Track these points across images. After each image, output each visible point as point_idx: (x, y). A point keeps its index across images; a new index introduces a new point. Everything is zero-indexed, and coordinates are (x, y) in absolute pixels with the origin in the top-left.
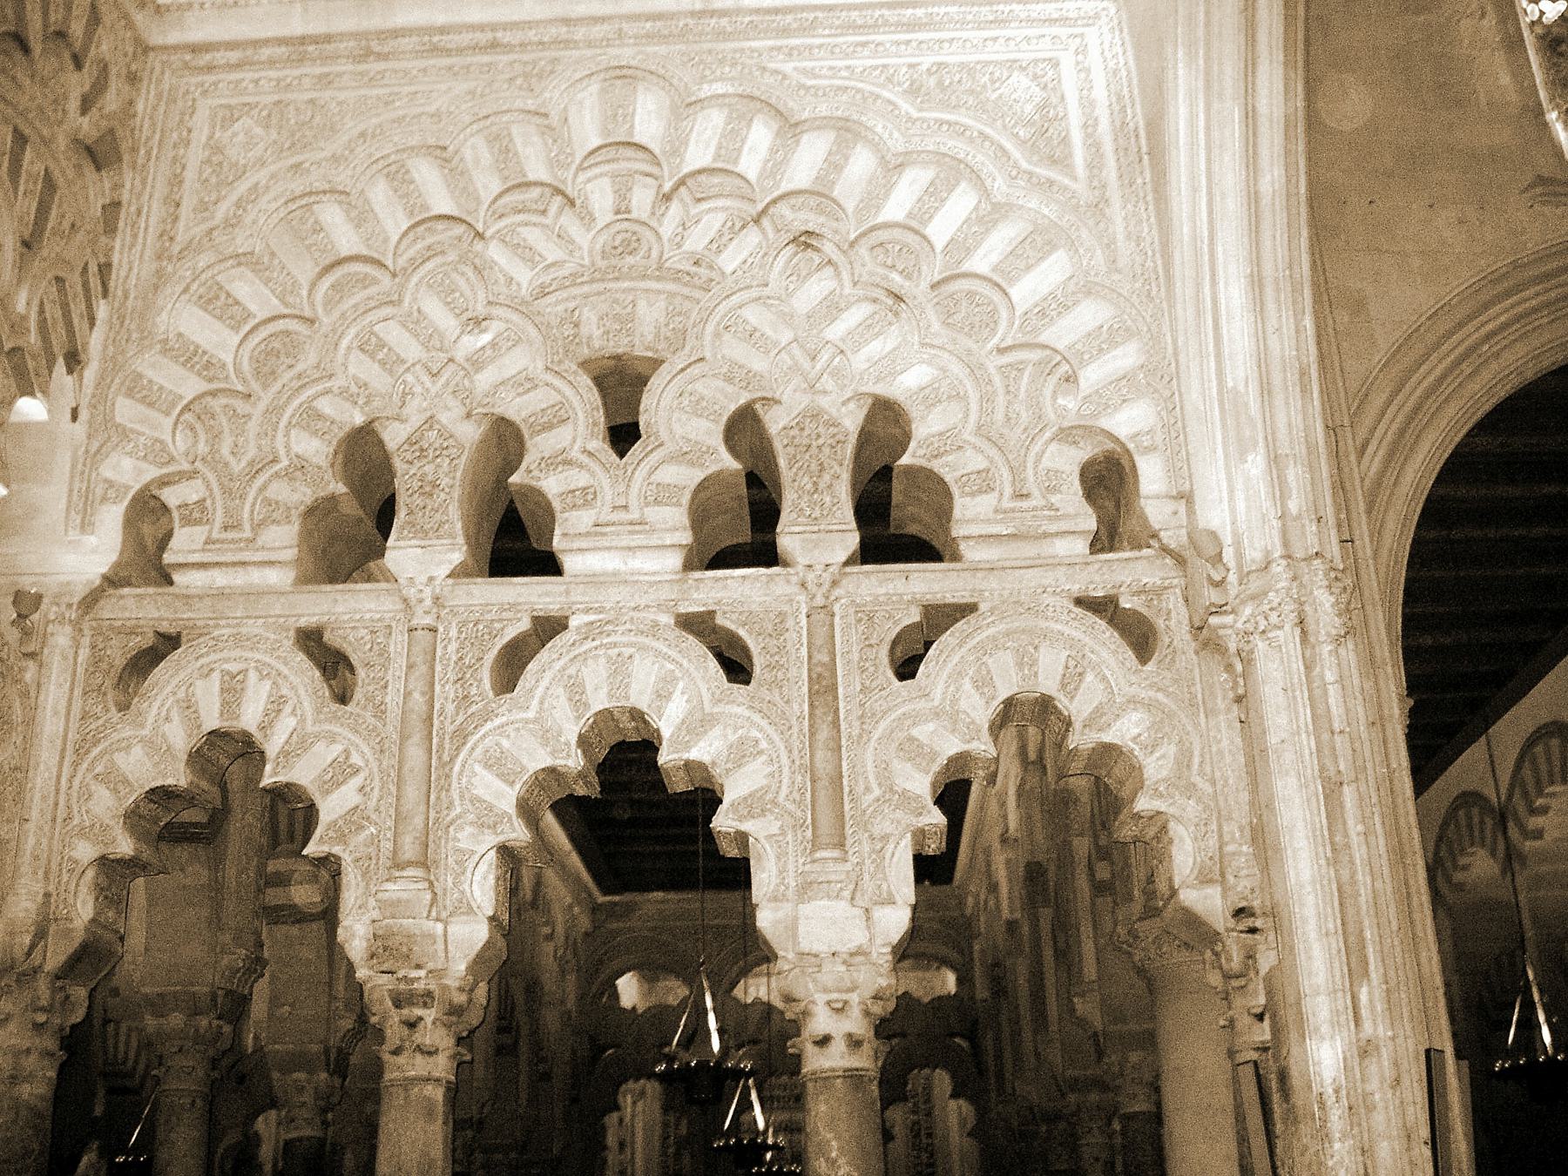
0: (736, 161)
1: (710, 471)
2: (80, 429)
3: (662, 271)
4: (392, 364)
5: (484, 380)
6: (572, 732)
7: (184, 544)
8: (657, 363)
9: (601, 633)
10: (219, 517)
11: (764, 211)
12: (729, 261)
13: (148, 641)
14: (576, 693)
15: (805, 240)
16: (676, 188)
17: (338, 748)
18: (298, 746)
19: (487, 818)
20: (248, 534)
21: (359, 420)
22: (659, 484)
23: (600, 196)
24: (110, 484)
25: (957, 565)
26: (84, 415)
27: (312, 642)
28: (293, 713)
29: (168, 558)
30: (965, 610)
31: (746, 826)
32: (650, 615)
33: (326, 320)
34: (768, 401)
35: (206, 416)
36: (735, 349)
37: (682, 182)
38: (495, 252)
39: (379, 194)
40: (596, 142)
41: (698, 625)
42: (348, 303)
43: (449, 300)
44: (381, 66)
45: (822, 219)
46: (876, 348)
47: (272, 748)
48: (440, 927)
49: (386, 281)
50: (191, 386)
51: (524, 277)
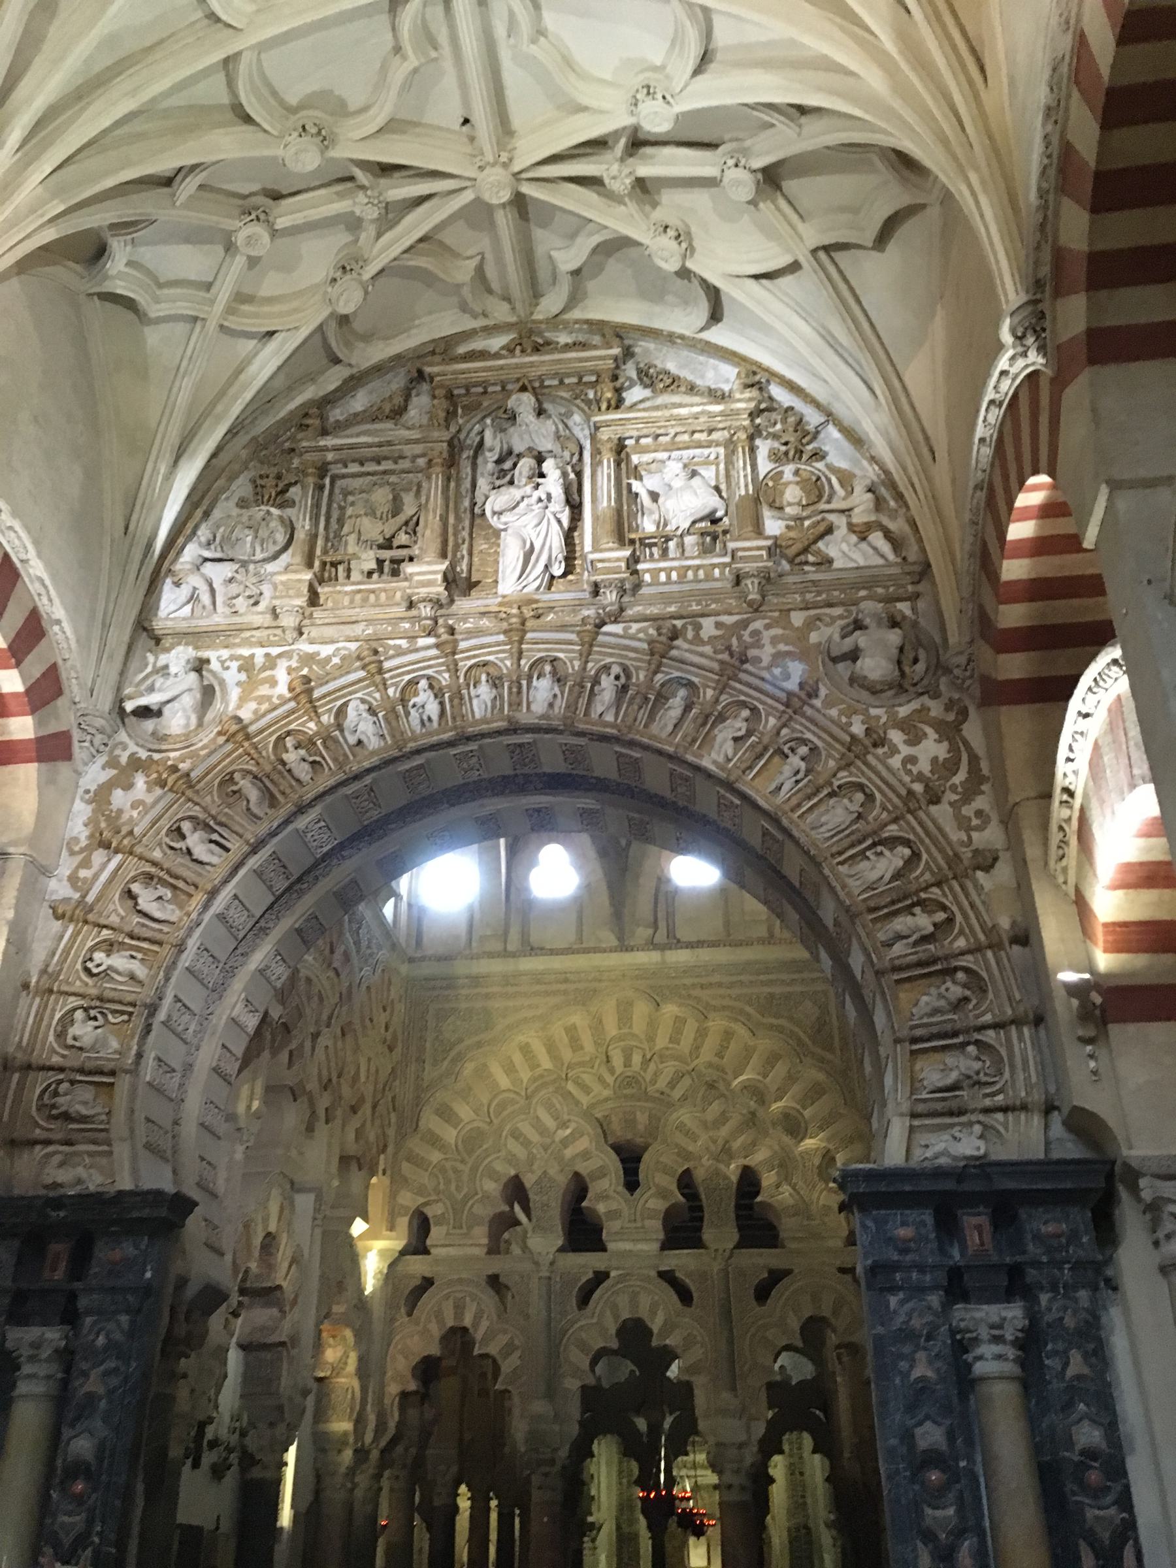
2: (386, 1180)
3: (646, 1097)
4: (526, 1143)
6: (613, 1331)
7: (436, 1234)
13: (418, 1282)
14: (615, 1308)
15: (711, 1086)
18: (489, 1336)
20: (464, 1231)
21: (513, 1173)
23: (618, 1061)
26: (388, 1172)
29: (429, 1242)
30: (788, 1273)
31: (693, 1379)
32: (645, 1272)
33: (495, 1121)
35: (443, 1170)
36: (680, 1139)
38: (570, 1086)
39: (517, 1058)
41: (667, 1277)
42: (505, 1113)
44: (515, 989)
47: (479, 1336)
48: (556, 1428)
49: (522, 1102)
50: (435, 1156)
51: (585, 1100)
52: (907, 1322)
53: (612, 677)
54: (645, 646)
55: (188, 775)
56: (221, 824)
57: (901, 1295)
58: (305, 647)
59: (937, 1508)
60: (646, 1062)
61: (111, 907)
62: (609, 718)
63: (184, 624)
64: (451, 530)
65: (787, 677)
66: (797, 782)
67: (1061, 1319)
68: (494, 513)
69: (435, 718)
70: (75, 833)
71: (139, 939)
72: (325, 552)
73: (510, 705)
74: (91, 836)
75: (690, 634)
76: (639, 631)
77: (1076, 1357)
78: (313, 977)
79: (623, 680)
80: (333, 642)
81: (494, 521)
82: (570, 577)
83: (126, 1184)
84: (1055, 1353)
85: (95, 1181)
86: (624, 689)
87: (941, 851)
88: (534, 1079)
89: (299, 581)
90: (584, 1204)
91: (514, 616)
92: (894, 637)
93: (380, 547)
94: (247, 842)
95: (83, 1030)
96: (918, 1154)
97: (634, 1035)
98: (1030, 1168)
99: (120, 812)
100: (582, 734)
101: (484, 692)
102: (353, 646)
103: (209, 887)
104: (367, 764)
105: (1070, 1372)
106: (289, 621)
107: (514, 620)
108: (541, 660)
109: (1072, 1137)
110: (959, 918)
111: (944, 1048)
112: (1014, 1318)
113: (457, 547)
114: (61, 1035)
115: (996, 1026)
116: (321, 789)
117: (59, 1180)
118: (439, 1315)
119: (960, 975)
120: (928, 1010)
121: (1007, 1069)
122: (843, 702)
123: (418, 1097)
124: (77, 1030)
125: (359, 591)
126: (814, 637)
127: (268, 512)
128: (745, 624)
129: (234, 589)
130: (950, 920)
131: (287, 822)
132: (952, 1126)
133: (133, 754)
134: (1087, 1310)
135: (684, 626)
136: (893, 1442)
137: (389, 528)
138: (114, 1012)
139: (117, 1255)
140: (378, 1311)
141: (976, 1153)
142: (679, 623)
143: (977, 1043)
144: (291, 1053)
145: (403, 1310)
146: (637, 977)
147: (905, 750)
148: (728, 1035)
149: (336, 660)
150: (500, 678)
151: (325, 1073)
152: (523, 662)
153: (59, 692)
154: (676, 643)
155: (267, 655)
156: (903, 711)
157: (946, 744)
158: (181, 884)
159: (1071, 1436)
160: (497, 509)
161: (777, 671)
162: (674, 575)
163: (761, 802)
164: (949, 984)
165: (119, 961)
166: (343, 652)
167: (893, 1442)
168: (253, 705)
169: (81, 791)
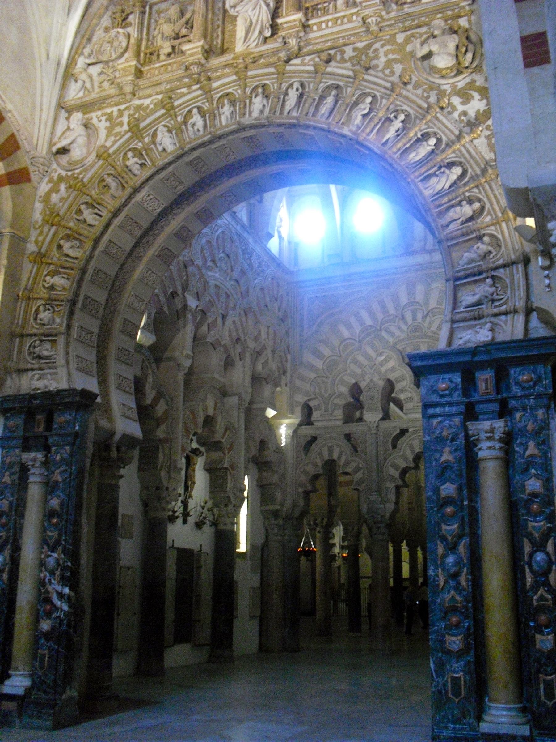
2: (287, 389)
3: (425, 336)
4: (361, 366)
6: (411, 457)
7: (316, 415)
10: (323, 408)
14: (411, 447)
16: (427, 314)
17: (356, 464)
19: (392, 479)
21: (354, 381)
23: (409, 317)
24: (296, 402)
26: (288, 385)
27: (348, 437)
29: (312, 419)
33: (343, 356)
38: (384, 334)
39: (353, 320)
42: (348, 351)
48: (382, 506)
49: (357, 344)
51: (391, 340)
52: (441, 433)
53: (295, 89)
54: (312, 68)
55: (82, 181)
56: (99, 204)
57: (440, 419)
58: (137, 102)
59: (448, 525)
60: (425, 317)
61: (52, 254)
62: (294, 114)
63: (79, 102)
64: (209, 22)
65: (393, 73)
66: (398, 135)
67: (527, 426)
68: (231, 7)
69: (201, 129)
70: (36, 219)
71: (64, 268)
72: (147, 47)
73: (240, 114)
74: (43, 219)
75: (339, 57)
76: (309, 61)
77: (531, 444)
78: (218, 283)
79: (300, 90)
80: (150, 96)
81: (232, 12)
82: (275, 36)
83: (64, 386)
84: (521, 444)
85: (53, 386)
86: (301, 95)
87: (479, 165)
88: (362, 331)
89: (130, 66)
91: (241, 63)
92: (452, 42)
93: (175, 38)
94: (110, 211)
95: (44, 315)
96: (458, 343)
98: (513, 345)
99: (55, 205)
100: (280, 125)
101: (227, 110)
102: (160, 97)
103: (94, 237)
104: (166, 161)
105: (528, 453)
106: (128, 89)
107: (241, 66)
108: (256, 87)
109: (543, 326)
110: (488, 206)
111: (475, 282)
112: (500, 427)
113: (213, 30)
114: (35, 319)
115: (505, 266)
116: (144, 178)
117: (37, 387)
118: (321, 454)
119: (486, 239)
120: (465, 260)
121: (509, 291)
122: (425, 84)
123: (301, 346)
124: (41, 315)
125: (162, 66)
126: (409, 48)
127: (118, 32)
128: (369, 46)
129: (103, 77)
130: (483, 208)
131: (130, 198)
132: (476, 325)
133: (59, 175)
134: (541, 420)
135: (335, 54)
136: (430, 493)
137: (176, 28)
138: (57, 305)
139: (62, 419)
140: (290, 455)
141: (486, 339)
142: (332, 52)
143: (493, 277)
144: (208, 325)
145: (303, 454)
146: (418, 270)
147: (461, 108)
149: (152, 106)
150: (235, 101)
151: (234, 334)
152: (247, 90)
153: (18, 148)
154: (330, 64)
155: (119, 110)
156: (460, 85)
157: (485, 101)
158: (82, 238)
159: (524, 486)
160: (232, 4)
161: (387, 72)
162: (330, 24)
163: (376, 150)
164: (479, 244)
165: (57, 280)
166: (155, 101)
167: (430, 493)
168: (112, 138)
169: (37, 197)
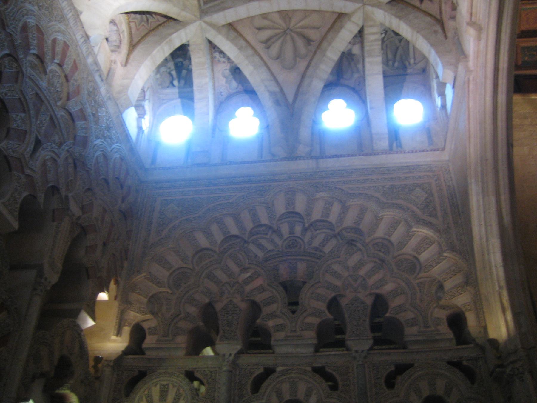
0: (328, 217)
1: (324, 318)
2: (116, 303)
5: (248, 288)
7: (149, 341)
8: (304, 283)
9: (287, 373)
11: (339, 234)
12: (327, 249)
13: (137, 373)
15: (351, 243)
21: (207, 300)
22: (306, 323)
23: (285, 230)
25: (407, 351)
28: (184, 399)
29: (144, 346)
34: (342, 296)
36: (329, 278)
37: (311, 225)
39: (214, 228)
40: (283, 211)
41: (320, 371)
43: (236, 262)
44: (215, 188)
45: (356, 236)
46: (376, 278)
60: (305, 230)
88: (223, 242)
90: (258, 321)
97: (297, 213)
148: (363, 210)
